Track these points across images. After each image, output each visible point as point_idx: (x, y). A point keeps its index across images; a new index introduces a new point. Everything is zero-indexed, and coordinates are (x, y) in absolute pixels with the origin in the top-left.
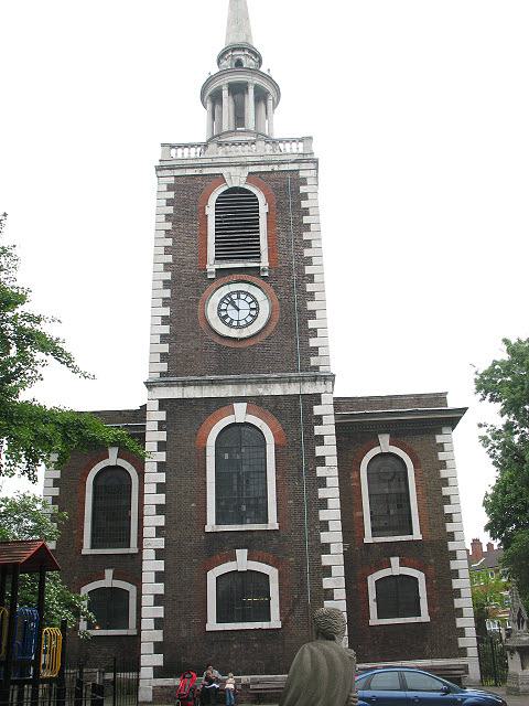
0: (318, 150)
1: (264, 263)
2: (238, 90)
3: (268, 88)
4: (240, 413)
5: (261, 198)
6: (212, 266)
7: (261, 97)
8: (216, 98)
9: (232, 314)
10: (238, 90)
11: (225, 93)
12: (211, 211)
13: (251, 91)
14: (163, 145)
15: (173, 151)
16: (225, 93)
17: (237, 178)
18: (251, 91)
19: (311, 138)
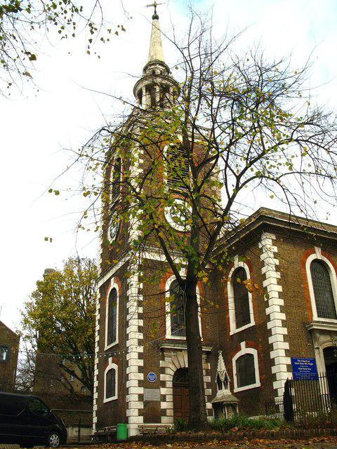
8: (150, 89)
16: (158, 89)
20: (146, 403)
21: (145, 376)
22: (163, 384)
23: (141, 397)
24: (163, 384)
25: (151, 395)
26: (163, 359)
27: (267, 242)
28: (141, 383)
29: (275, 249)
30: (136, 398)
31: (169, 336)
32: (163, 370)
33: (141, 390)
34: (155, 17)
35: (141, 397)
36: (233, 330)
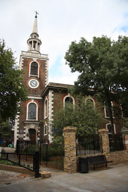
0: (49, 57)
1: (38, 77)
2: (35, 42)
3: (40, 43)
4: (32, 101)
5: (39, 64)
6: (30, 75)
7: (39, 44)
8: (31, 43)
9: (33, 84)
10: (35, 42)
11: (33, 42)
12: (30, 65)
13: (37, 43)
14: (22, 51)
15: (24, 52)
16: (33, 42)
17: (35, 60)
18: (37, 43)
19: (48, 55)
20: (19, 138)
21: (19, 131)
22: (25, 133)
23: (18, 137)
24: (25, 133)
25: (21, 136)
26: (25, 126)
27: (50, 94)
28: (18, 133)
29: (53, 95)
30: (16, 137)
31: (27, 120)
32: (25, 129)
33: (18, 135)
34: (36, 17)
35: (18, 137)
36: (45, 118)
